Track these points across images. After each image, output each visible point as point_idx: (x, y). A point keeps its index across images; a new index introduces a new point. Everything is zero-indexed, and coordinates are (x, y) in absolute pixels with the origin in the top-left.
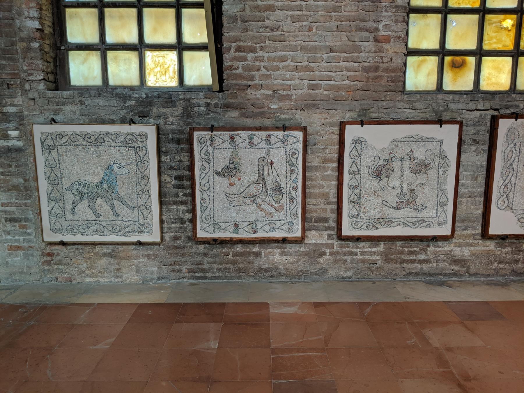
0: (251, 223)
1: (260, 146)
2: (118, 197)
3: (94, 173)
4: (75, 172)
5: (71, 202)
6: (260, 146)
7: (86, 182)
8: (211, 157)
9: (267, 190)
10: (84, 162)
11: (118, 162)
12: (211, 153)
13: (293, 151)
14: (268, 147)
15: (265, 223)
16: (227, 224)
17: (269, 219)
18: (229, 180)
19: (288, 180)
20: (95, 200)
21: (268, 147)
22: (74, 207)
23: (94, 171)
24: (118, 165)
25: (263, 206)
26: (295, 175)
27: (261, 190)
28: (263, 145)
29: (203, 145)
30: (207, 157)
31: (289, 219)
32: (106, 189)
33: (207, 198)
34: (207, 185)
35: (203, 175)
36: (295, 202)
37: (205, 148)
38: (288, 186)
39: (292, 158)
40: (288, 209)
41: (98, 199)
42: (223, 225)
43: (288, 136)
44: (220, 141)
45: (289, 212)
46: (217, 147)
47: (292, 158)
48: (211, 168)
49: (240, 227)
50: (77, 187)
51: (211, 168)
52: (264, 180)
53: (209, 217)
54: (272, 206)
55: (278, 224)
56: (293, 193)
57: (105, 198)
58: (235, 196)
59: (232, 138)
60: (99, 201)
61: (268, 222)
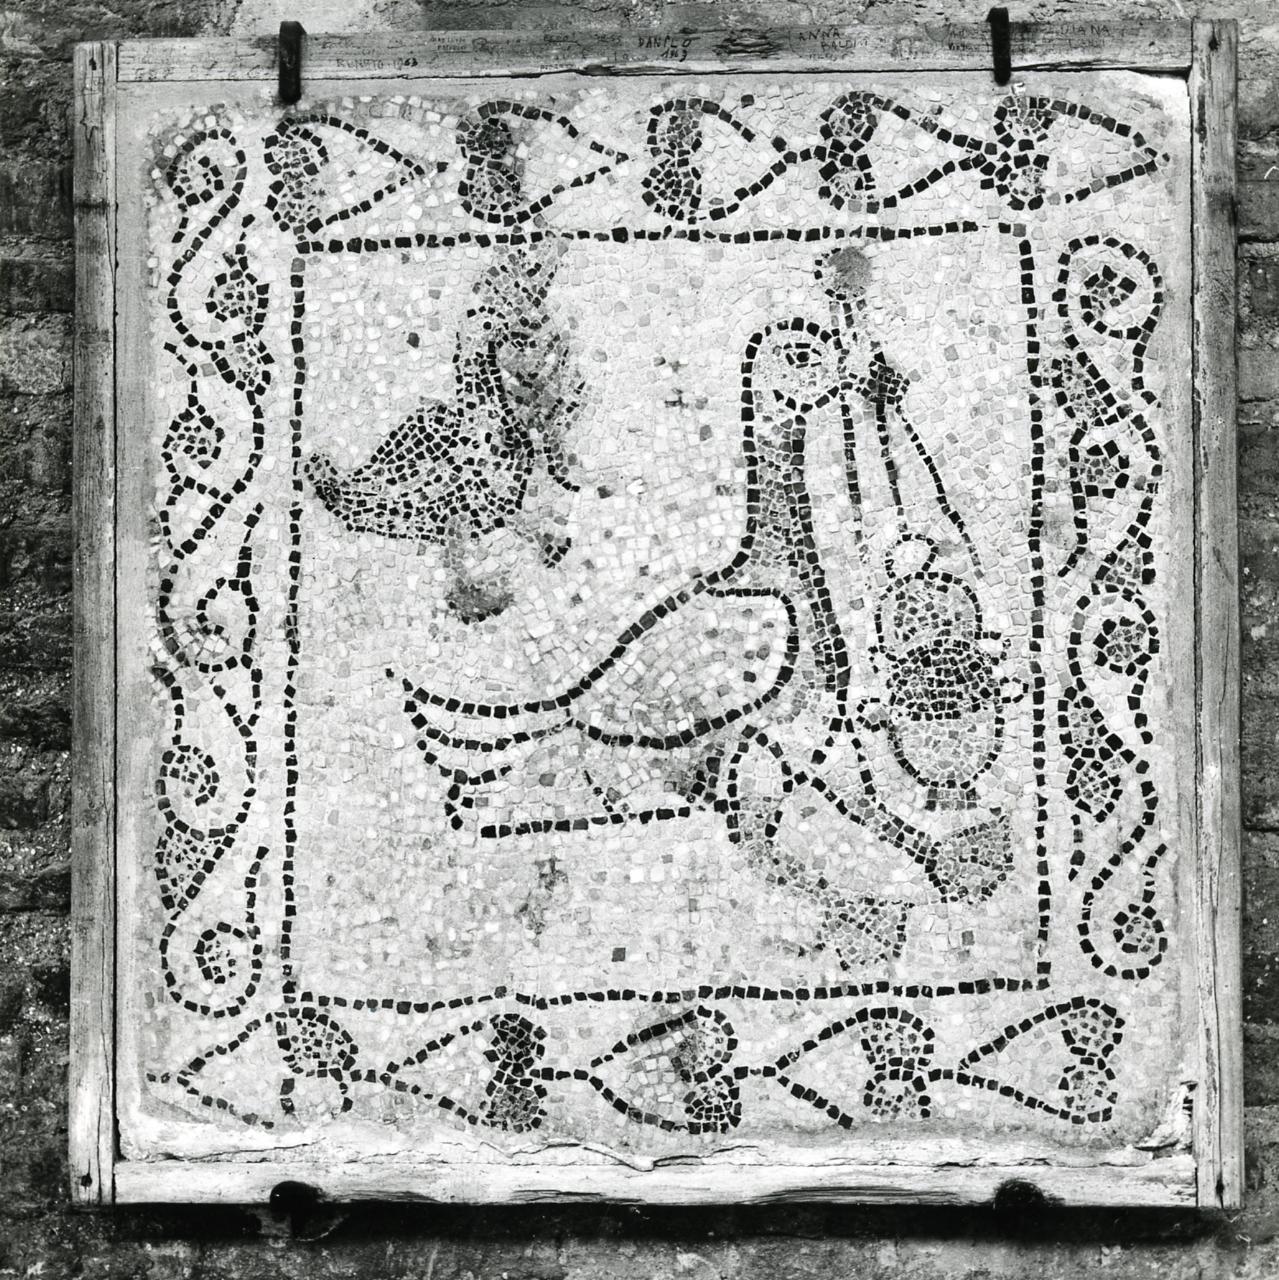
0: (669, 1021)
1: (765, 211)
6: (765, 211)
8: (276, 332)
9: (836, 658)
12: (281, 295)
13: (1093, 258)
14: (843, 219)
15: (816, 1017)
16: (423, 1028)
17: (857, 978)
18: (450, 561)
19: (1053, 553)
21: (843, 219)
25: (793, 835)
26: (1123, 508)
27: (777, 660)
28: (797, 198)
29: (201, 214)
30: (237, 325)
31: (1072, 978)
33: (227, 749)
34: (228, 606)
35: (192, 509)
36: (1132, 786)
37: (226, 236)
38: (1058, 625)
39: (1084, 332)
40: (1059, 863)
42: (382, 1038)
43: (1042, 112)
44: (377, 169)
45: (1068, 896)
46: (338, 231)
47: (1084, 332)
48: (278, 441)
49: (554, 1055)
51: (278, 441)
52: (805, 553)
53: (241, 949)
54: (897, 832)
55: (957, 1028)
56: (1108, 689)
58: (511, 726)
59: (490, 137)
61: (848, 1005)
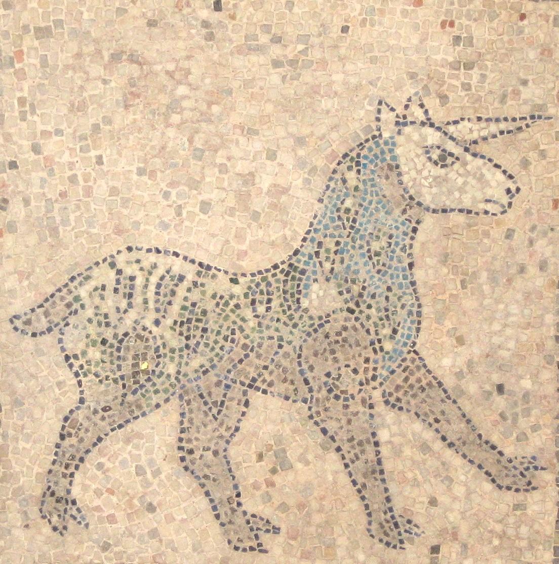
2: (417, 390)
3: (243, 198)
4: (101, 188)
5: (51, 426)
7: (178, 266)
10: (174, 106)
11: (438, 115)
20: (234, 409)
22: (69, 459)
23: (249, 178)
24: (432, 137)
32: (326, 319)
41: (256, 398)
50: (110, 303)
57: (319, 398)
60: (269, 417)
